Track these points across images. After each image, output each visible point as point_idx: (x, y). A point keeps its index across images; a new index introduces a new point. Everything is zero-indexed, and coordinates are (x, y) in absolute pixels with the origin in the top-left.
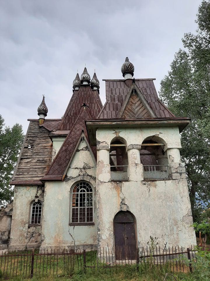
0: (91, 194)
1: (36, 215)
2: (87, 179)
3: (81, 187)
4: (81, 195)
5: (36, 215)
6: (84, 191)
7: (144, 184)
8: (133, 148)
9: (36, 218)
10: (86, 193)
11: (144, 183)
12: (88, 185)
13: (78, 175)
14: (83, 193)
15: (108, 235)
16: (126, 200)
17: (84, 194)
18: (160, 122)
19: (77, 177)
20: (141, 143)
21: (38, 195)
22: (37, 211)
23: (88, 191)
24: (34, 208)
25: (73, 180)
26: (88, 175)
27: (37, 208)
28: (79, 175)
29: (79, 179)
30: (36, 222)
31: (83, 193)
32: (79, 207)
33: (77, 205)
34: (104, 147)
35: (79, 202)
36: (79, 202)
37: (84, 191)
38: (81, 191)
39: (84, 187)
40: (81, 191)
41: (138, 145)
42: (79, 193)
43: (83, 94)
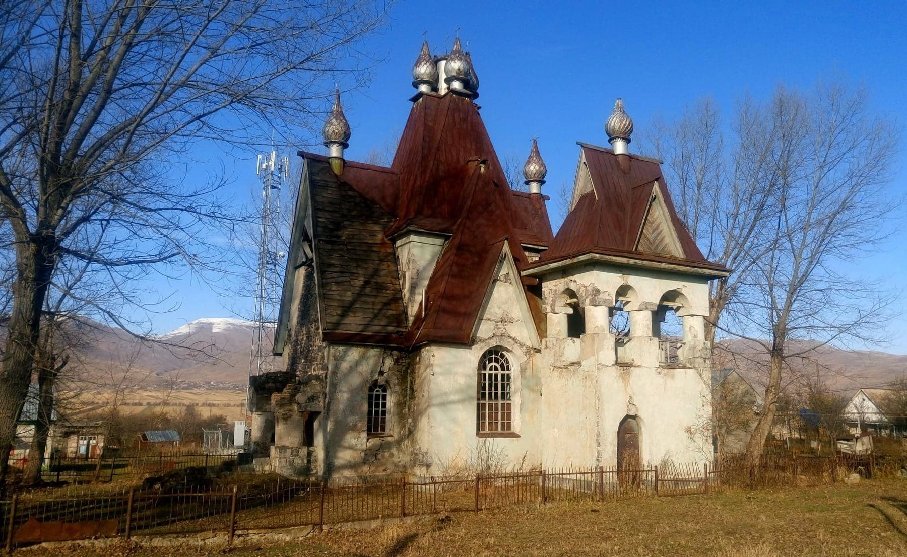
0: (509, 377)
1: (377, 413)
2: (507, 344)
3: (490, 361)
4: (490, 375)
5: (377, 413)
6: (496, 369)
7: (659, 373)
8: (647, 309)
9: (377, 420)
10: (500, 372)
11: (659, 370)
12: (503, 356)
13: (491, 334)
14: (493, 372)
15: (610, 453)
16: (635, 398)
17: (496, 375)
18: (693, 269)
19: (490, 338)
20: (657, 302)
21: (386, 368)
22: (377, 405)
23: (503, 369)
24: (370, 397)
25: (482, 344)
26: (510, 337)
27: (378, 397)
28: (494, 336)
29: (493, 343)
30: (376, 429)
31: (493, 372)
32: (487, 402)
33: (484, 395)
34: (605, 301)
35: (487, 392)
36: (487, 392)
37: (496, 369)
38: (491, 369)
39: (497, 361)
40: (491, 369)
41: (652, 304)
42: (487, 372)
43: (456, 115)
